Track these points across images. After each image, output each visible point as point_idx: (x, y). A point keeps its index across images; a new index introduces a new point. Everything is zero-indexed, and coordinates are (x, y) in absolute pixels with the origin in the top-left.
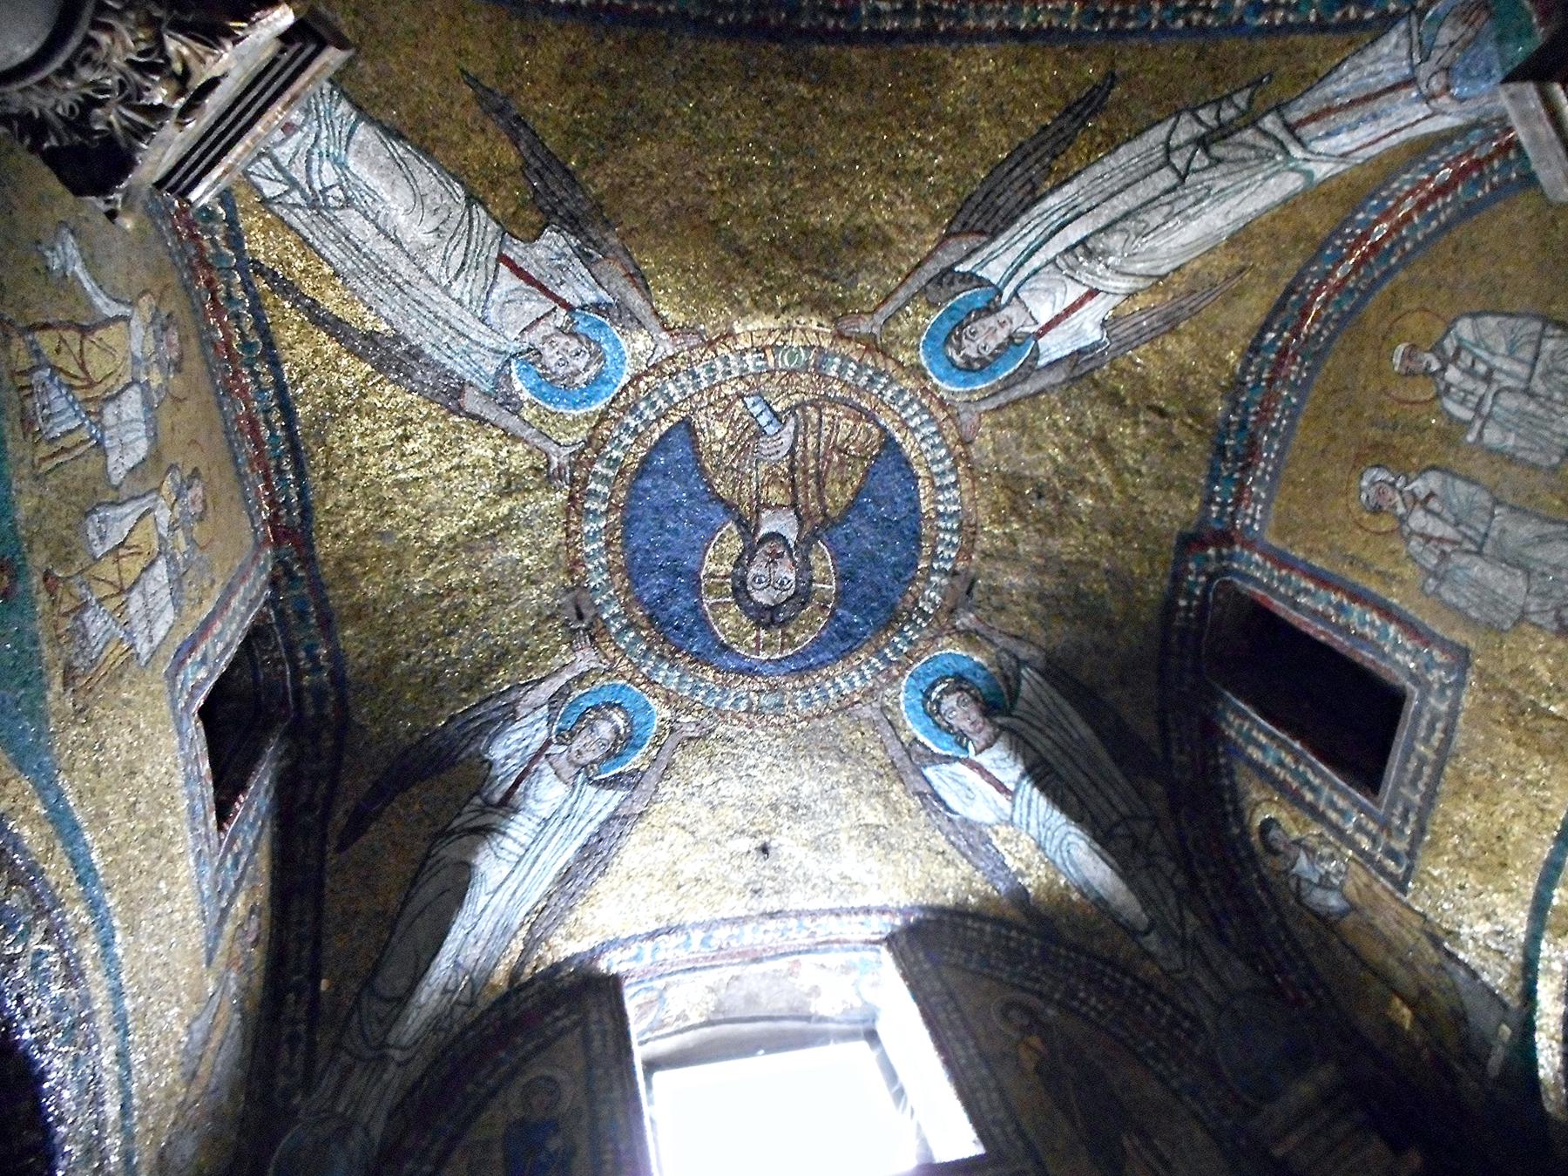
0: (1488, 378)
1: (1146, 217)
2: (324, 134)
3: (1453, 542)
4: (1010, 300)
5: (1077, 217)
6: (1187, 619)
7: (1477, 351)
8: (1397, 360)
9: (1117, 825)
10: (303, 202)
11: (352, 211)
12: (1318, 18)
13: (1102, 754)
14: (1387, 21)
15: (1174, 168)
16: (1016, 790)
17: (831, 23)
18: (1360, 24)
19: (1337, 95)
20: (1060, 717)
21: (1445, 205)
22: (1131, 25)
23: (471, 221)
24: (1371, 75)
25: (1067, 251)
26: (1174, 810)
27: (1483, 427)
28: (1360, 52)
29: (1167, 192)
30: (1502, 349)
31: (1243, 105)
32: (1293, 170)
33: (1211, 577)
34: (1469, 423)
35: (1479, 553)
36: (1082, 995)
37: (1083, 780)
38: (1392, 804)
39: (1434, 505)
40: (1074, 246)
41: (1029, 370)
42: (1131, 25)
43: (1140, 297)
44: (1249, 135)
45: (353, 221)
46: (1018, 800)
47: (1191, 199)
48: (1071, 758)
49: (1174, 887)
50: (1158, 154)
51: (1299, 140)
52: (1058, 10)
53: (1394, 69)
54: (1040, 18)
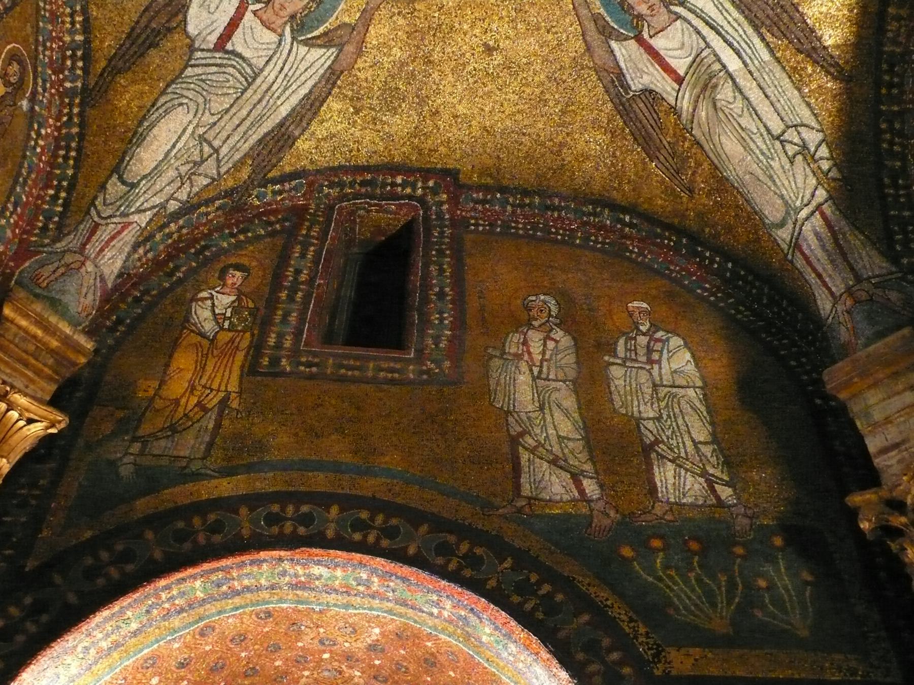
0: (650, 362)
3: (532, 359)
4: (676, 13)
5: (744, 63)
6: (384, 185)
7: (665, 351)
8: (636, 304)
9: (210, 144)
12: (894, 216)
13: (267, 126)
14: (894, 259)
15: (784, 132)
16: (227, 52)
19: (844, 234)
20: (294, 87)
21: (746, 316)
22: (884, 91)
25: (716, 55)
26: (229, 194)
27: (617, 364)
30: (674, 366)
31: (831, 175)
32: (788, 213)
33: (422, 200)
34: (615, 356)
35: (534, 379)
36: (43, 132)
37: (244, 112)
38: (315, 355)
39: (551, 345)
40: (719, 60)
41: (606, 33)
43: (672, 118)
46: (217, 55)
47: (764, 147)
48: (260, 101)
49: (167, 201)
50: (791, 119)
51: (813, 213)
52: (899, 35)
53: (864, 267)
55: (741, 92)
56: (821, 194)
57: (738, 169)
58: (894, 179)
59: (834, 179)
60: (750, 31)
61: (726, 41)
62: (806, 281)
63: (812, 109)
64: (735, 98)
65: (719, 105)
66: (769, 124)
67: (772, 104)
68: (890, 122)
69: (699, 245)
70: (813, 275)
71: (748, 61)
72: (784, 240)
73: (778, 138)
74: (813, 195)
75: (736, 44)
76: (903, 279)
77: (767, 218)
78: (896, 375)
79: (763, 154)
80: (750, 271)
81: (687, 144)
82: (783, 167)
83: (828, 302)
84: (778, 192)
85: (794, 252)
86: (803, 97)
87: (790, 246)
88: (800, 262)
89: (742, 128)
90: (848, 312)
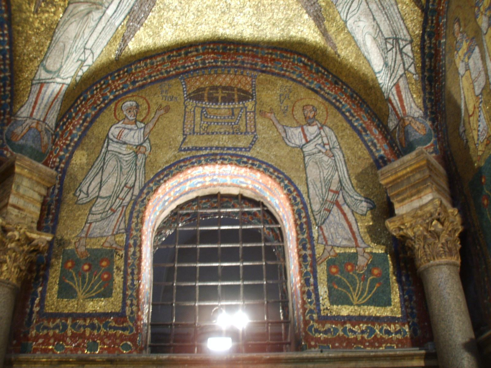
1: (90, 29)
2: (388, 79)
5: (112, 15)
10: (400, 41)
11: (386, 36)
12: (71, 111)
14: (57, 125)
17: (212, 46)
18: (61, 120)
19: (57, 101)
22: (116, 74)
23: (347, 17)
24: (53, 113)
28: (59, 114)
29: (87, 42)
32: (55, 72)
40: (110, 4)
42: (116, 74)
44: (73, 74)
45: (387, 33)
47: (79, 46)
51: (60, 83)
54: (143, 65)
55: (99, 22)
56: (69, 81)
57: (63, 37)
58: (84, 99)
59: (76, 80)
60: (127, 12)
61: (119, 3)
62: (29, 97)
63: (101, 54)
64: (96, 20)
65: (90, 15)
66: (89, 42)
67: (98, 37)
68: (104, 83)
69: (7, 24)
70: (34, 100)
71: (113, 17)
72: (40, 76)
73: (85, 48)
74: (67, 78)
75: (119, 8)
76: (52, 135)
77: (46, 62)
78: (38, 183)
79: (76, 47)
80: (12, 60)
81: (62, 4)
82: (74, 59)
83: (27, 114)
84: (63, 64)
85: (38, 83)
86: (105, 47)
87: (39, 80)
88: (36, 89)
89: (83, 32)
90: (30, 128)
